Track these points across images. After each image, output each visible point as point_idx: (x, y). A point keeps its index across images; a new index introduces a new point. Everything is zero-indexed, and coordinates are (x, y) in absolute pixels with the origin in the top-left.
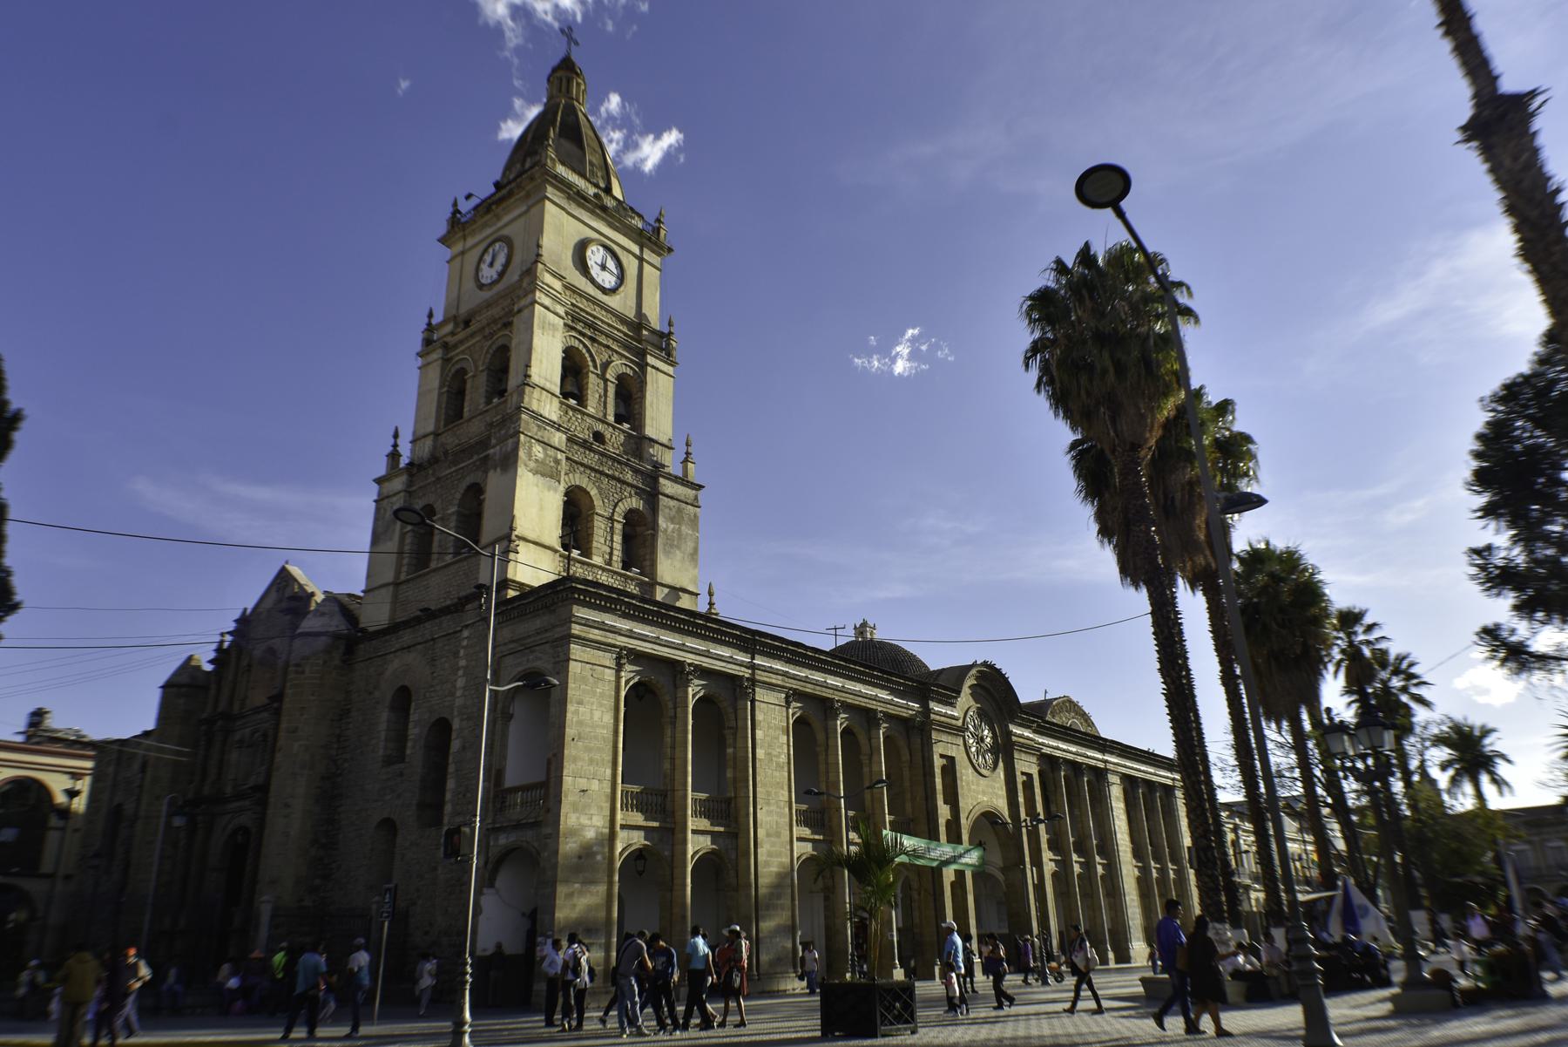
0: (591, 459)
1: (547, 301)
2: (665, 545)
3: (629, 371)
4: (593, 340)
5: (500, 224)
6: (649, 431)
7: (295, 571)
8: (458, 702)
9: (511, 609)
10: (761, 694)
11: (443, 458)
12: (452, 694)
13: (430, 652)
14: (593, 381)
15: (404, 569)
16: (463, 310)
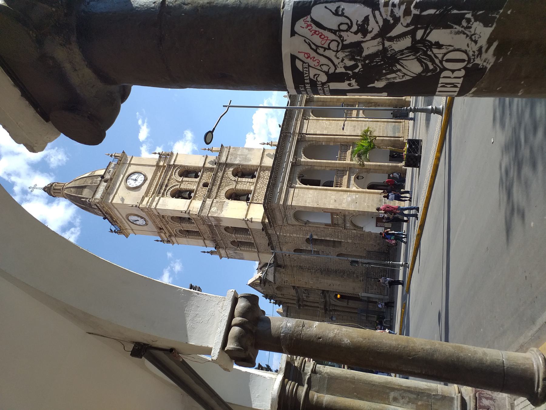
0: (215, 189)
1: (154, 204)
2: (246, 162)
3: (177, 172)
4: (167, 186)
5: (121, 217)
6: (201, 165)
7: (250, 281)
8: (301, 236)
9: (272, 221)
10: (304, 131)
11: (214, 238)
12: (298, 237)
13: (283, 243)
14: (183, 186)
15: (253, 250)
16: (156, 230)
